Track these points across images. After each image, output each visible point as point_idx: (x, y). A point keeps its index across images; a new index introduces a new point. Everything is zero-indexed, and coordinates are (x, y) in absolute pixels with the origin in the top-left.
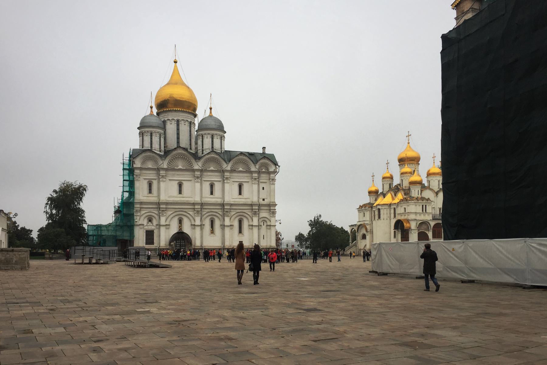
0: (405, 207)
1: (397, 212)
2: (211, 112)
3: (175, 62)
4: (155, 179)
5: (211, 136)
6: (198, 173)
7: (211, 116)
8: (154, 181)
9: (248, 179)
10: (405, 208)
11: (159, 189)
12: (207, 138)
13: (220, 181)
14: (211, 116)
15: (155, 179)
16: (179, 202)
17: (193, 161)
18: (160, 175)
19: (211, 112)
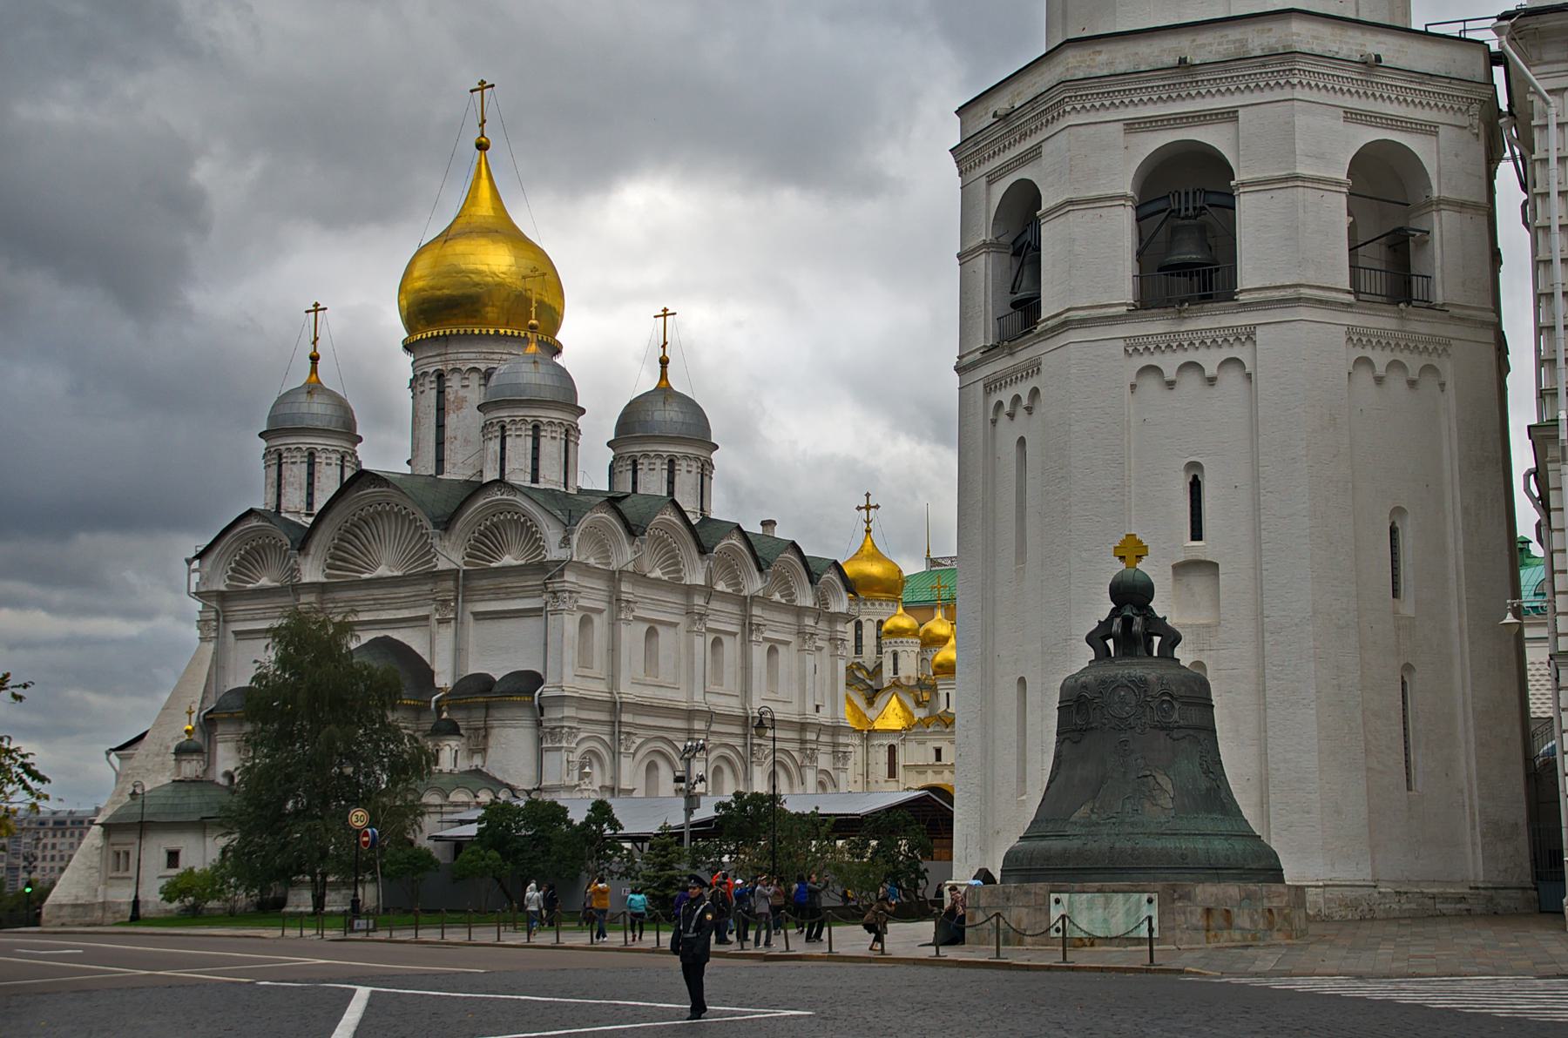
0: (938, 745)
1: (901, 759)
2: (664, 375)
3: (482, 147)
4: (600, 611)
5: (666, 461)
6: (699, 601)
7: (664, 390)
8: (596, 619)
9: (790, 633)
10: (938, 751)
11: (613, 649)
12: (689, 472)
13: (734, 634)
14: (664, 390)
15: (600, 611)
16: (656, 702)
17: (688, 552)
18: (618, 600)
19: (664, 375)
